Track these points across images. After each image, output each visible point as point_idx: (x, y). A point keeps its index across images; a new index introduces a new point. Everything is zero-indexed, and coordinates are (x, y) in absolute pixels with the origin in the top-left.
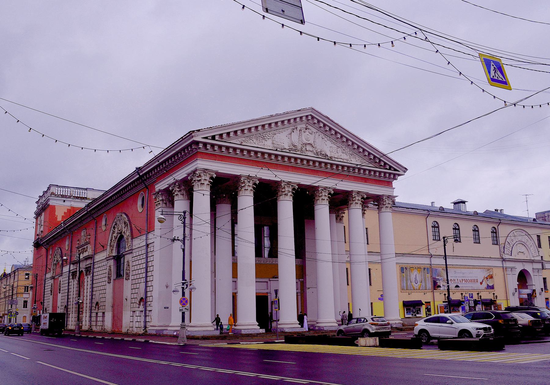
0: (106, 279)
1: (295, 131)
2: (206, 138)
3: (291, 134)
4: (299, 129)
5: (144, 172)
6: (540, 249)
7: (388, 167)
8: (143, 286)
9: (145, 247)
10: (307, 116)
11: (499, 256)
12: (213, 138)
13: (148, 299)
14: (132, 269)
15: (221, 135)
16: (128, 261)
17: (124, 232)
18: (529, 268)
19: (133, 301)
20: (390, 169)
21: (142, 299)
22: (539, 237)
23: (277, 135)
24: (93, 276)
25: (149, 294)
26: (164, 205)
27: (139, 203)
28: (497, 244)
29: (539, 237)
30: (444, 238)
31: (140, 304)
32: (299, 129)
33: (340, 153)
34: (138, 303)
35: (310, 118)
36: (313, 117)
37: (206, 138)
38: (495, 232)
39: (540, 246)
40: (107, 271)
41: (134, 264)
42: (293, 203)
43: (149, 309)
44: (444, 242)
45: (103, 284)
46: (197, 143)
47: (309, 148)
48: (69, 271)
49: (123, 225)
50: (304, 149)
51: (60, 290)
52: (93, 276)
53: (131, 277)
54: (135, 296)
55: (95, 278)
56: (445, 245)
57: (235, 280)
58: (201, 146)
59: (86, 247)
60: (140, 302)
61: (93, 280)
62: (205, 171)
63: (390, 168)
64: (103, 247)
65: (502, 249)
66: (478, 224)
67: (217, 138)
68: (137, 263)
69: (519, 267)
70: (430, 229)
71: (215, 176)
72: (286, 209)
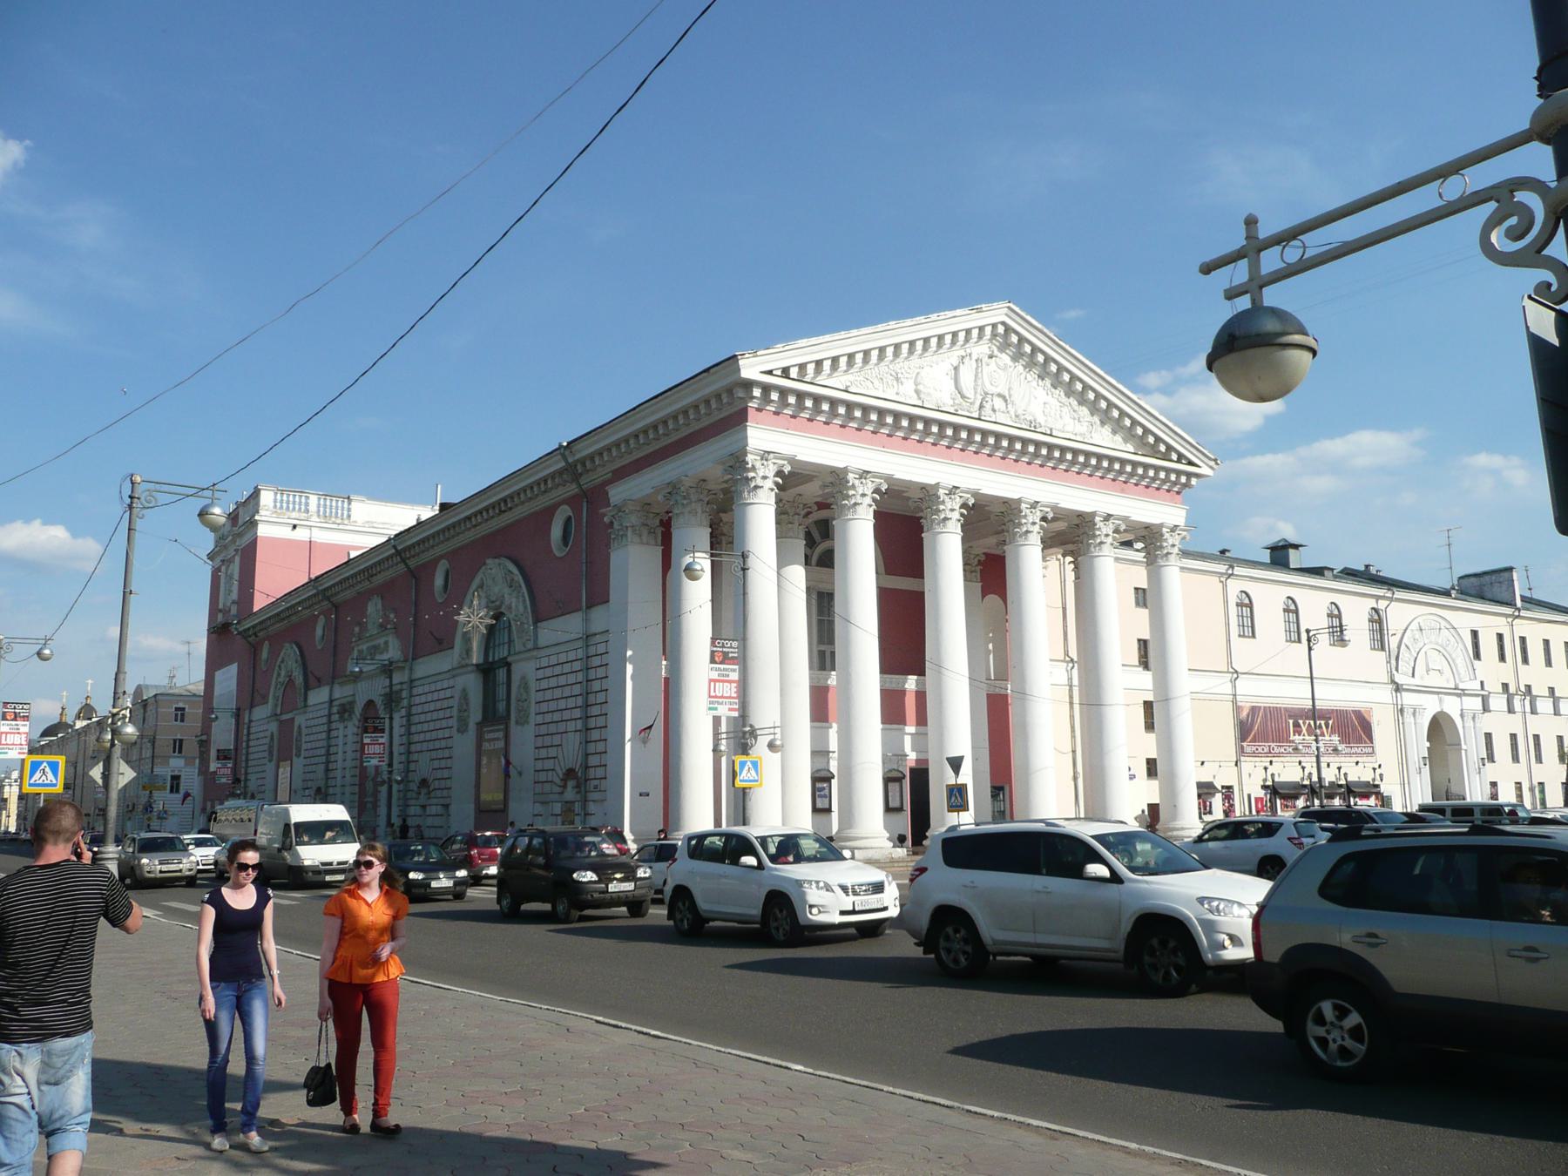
0: (453, 722)
1: (966, 360)
2: (770, 372)
3: (956, 369)
4: (975, 357)
5: (578, 456)
6: (1476, 663)
7: (1174, 456)
8: (572, 743)
9: (579, 644)
10: (994, 326)
11: (1386, 679)
12: (785, 372)
13: (592, 773)
14: (534, 697)
15: (802, 367)
16: (523, 678)
17: (510, 608)
18: (1452, 706)
19: (543, 777)
20: (1179, 461)
21: (570, 773)
22: (1475, 634)
23: (927, 369)
24: (409, 715)
25: (593, 760)
26: (637, 539)
27: (556, 532)
28: (1383, 649)
29: (1475, 634)
30: (1308, 631)
31: (565, 787)
32: (975, 357)
33: (1067, 419)
34: (558, 781)
35: (1001, 329)
36: (1008, 329)
37: (770, 372)
38: (1377, 621)
39: (1477, 656)
40: (455, 703)
41: (544, 684)
42: (963, 539)
43: (593, 796)
44: (1309, 640)
45: (447, 733)
46: (748, 385)
47: (999, 403)
48: (331, 701)
49: (507, 590)
50: (988, 406)
51: (299, 749)
52: (409, 715)
53: (533, 719)
54: (549, 764)
55: (415, 719)
56: (1310, 649)
57: (922, 729)
58: (757, 392)
59: (382, 641)
60: (565, 780)
61: (409, 724)
62: (765, 455)
63: (1181, 457)
64: (440, 641)
65: (1393, 662)
66: (1341, 600)
67: (794, 373)
68: (553, 682)
69: (1431, 706)
70: (1233, 610)
71: (787, 469)
72: (948, 553)
